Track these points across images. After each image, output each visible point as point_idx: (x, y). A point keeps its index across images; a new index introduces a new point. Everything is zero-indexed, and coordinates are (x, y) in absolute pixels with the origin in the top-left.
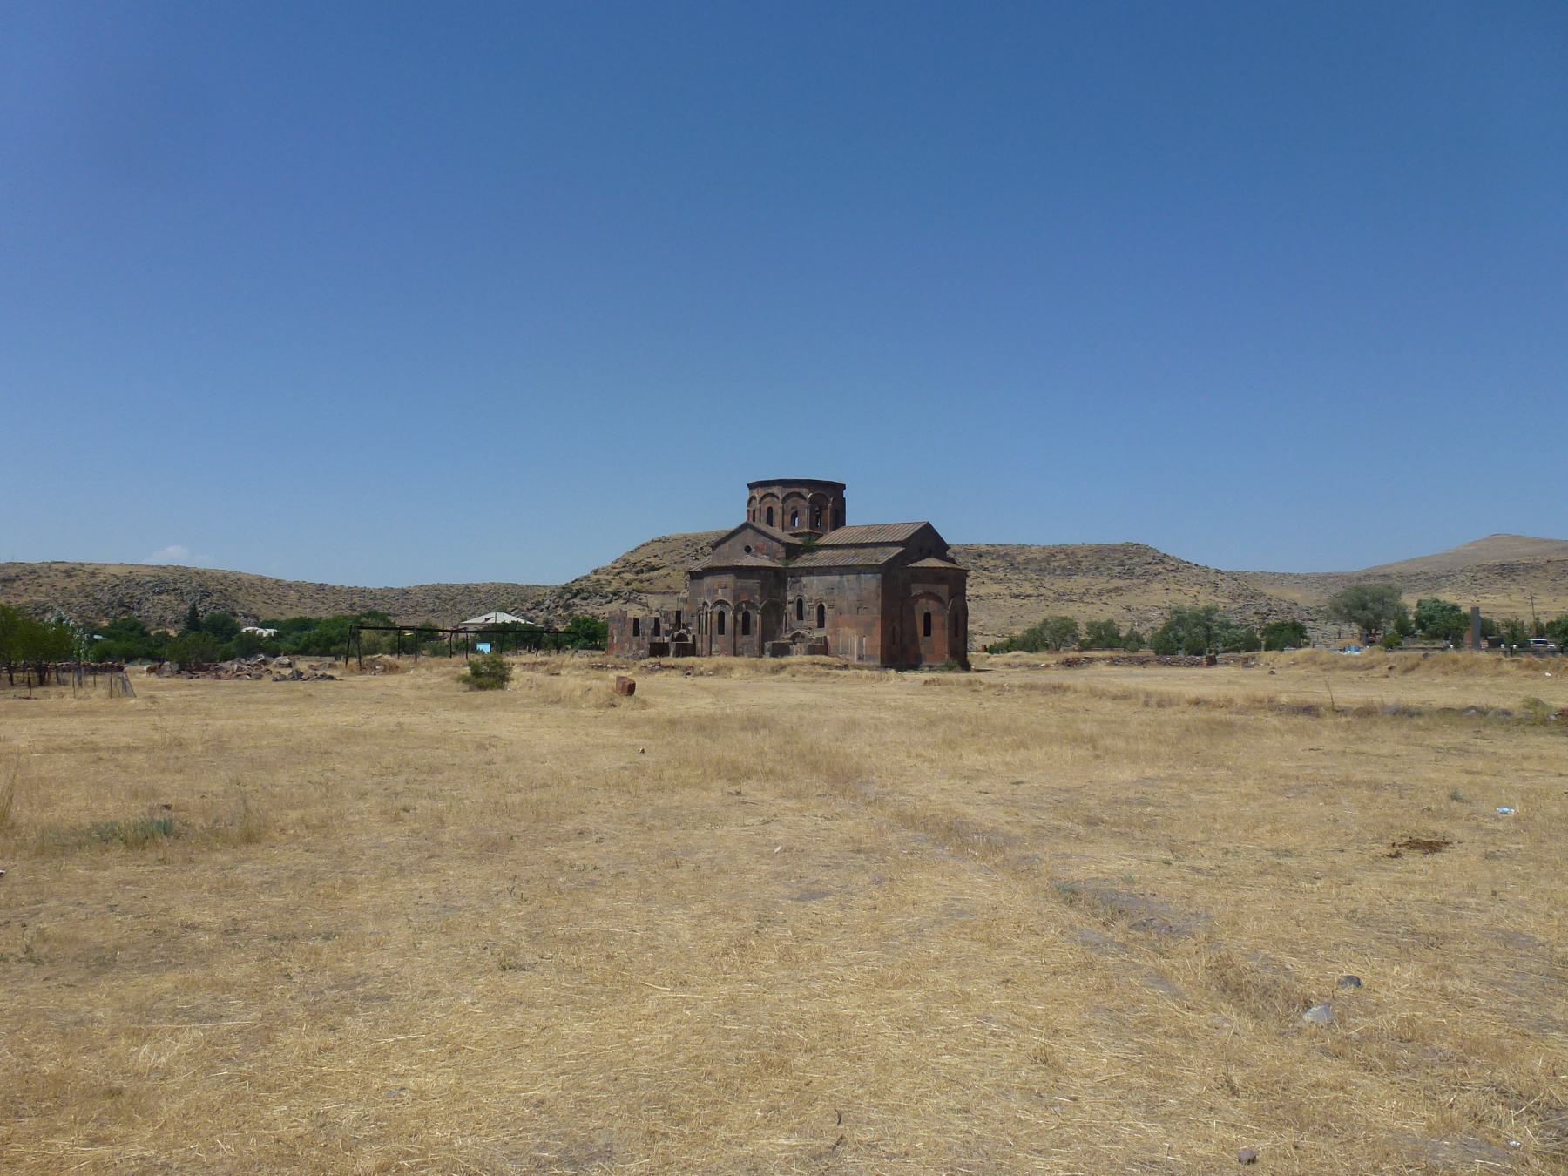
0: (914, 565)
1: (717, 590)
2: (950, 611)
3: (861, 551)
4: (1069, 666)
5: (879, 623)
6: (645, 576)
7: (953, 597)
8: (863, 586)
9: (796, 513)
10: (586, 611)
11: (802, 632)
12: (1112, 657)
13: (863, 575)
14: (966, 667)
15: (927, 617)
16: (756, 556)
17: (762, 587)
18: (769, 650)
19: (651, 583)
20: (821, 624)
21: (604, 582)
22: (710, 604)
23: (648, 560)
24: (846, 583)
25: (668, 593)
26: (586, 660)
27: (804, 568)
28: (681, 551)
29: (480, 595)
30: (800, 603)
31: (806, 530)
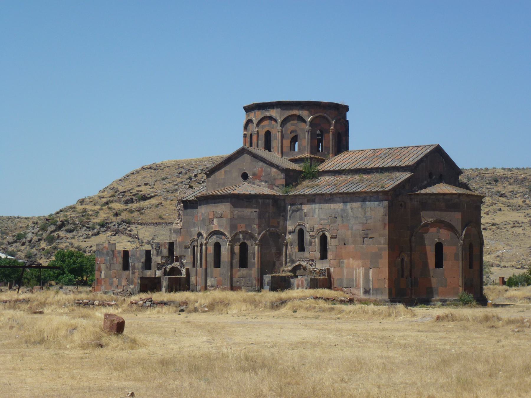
0: (423, 191)
1: (213, 220)
2: (463, 240)
3: (365, 177)
6: (135, 205)
7: (466, 225)
8: (368, 214)
9: (296, 136)
10: (72, 244)
11: (304, 264)
13: (367, 203)
14: (482, 301)
15: (439, 247)
16: (254, 183)
17: (261, 216)
18: (268, 284)
19: (141, 214)
20: (324, 256)
21: (90, 213)
22: (205, 235)
23: (140, 189)
24: (350, 211)
25: (160, 223)
26: (71, 296)
27: (304, 195)
30: (301, 233)
31: (307, 155)
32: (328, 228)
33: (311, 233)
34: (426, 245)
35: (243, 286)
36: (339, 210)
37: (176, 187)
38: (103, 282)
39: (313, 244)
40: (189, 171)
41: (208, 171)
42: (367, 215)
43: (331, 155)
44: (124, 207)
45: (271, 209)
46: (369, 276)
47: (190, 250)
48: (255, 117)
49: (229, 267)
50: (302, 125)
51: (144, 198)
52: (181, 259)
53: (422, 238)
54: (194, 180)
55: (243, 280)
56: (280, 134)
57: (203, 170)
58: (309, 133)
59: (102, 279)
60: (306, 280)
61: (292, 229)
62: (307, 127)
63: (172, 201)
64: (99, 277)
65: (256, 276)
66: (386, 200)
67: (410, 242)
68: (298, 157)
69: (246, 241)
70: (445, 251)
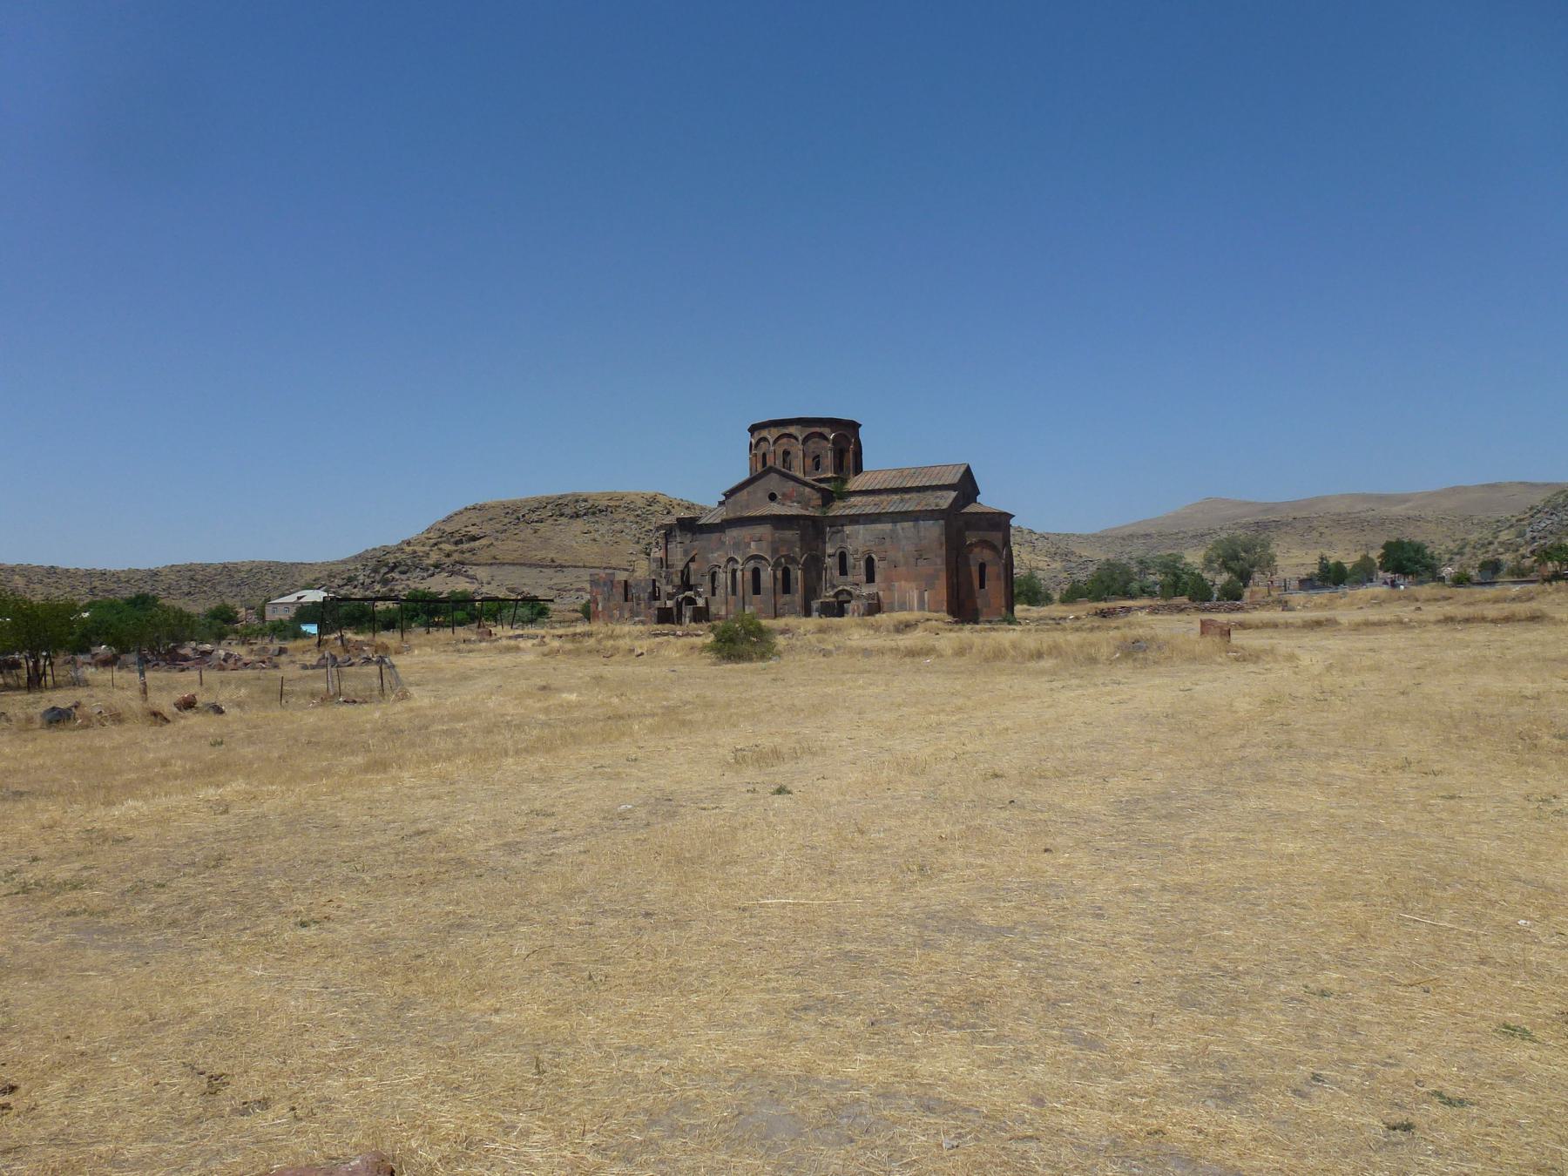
4: (1104, 617)
5: (943, 575)
6: (466, 546)
8: (922, 534)
10: (408, 585)
12: (1151, 606)
13: (922, 522)
15: (982, 567)
16: (783, 504)
17: (802, 538)
19: (474, 554)
20: (870, 578)
21: (421, 554)
23: (467, 529)
24: (900, 531)
25: (495, 564)
27: (847, 516)
29: (243, 575)
30: (843, 557)
31: (830, 475)
36: (888, 531)
37: (505, 527)
44: (454, 548)
47: (708, 578)
48: (769, 434)
51: (474, 539)
52: (696, 588)
55: (786, 607)
60: (863, 605)
66: (942, 519)
68: (822, 476)
69: (788, 566)
70: (987, 570)
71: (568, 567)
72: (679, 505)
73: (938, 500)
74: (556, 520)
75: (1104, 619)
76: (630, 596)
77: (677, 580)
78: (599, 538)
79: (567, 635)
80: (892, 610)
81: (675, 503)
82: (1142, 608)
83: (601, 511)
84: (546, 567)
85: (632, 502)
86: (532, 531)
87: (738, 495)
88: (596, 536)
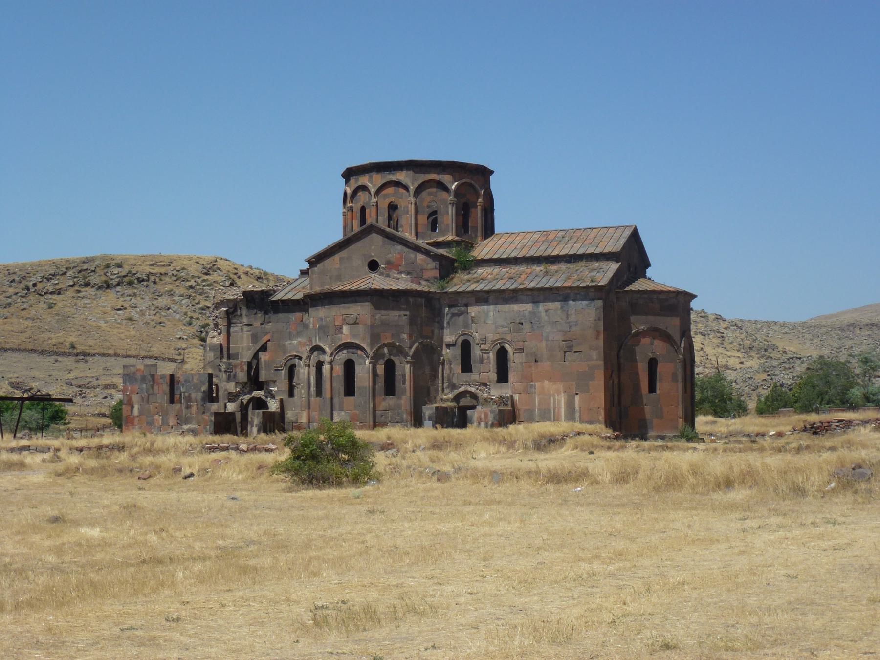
1: (341, 328)
4: (815, 433)
8: (572, 318)
13: (571, 302)
15: (653, 364)
16: (388, 276)
17: (412, 322)
18: (430, 419)
20: (503, 376)
24: (543, 314)
27: (473, 293)
28: (5, 288)
30: (466, 347)
31: (450, 237)
32: (509, 339)
33: (482, 346)
34: (638, 360)
35: (390, 422)
36: (527, 313)
37: (9, 300)
38: (136, 421)
39: (485, 361)
40: (24, 279)
41: (313, 258)
42: (570, 319)
43: (479, 239)
45: (424, 312)
46: (574, 404)
47: (284, 373)
48: (370, 181)
49: (371, 395)
50: (444, 194)
52: (268, 385)
53: (633, 353)
54: (33, 290)
55: (390, 413)
56: (413, 206)
57: (43, 277)
58: (454, 206)
59: (134, 417)
61: (451, 340)
62: (451, 198)
63: (6, 318)
64: (129, 413)
65: (408, 408)
67: (619, 358)
68: (440, 239)
69: (392, 358)
71: (94, 355)
72: (247, 273)
73: (594, 273)
74: (79, 292)
75: (814, 436)
76: (177, 397)
77: (242, 376)
78: (136, 317)
79: (90, 448)
80: (531, 419)
81: (240, 271)
82: (865, 423)
83: (140, 280)
84: (64, 354)
85: (183, 269)
86: (45, 306)
87: (328, 263)
88: (133, 313)
